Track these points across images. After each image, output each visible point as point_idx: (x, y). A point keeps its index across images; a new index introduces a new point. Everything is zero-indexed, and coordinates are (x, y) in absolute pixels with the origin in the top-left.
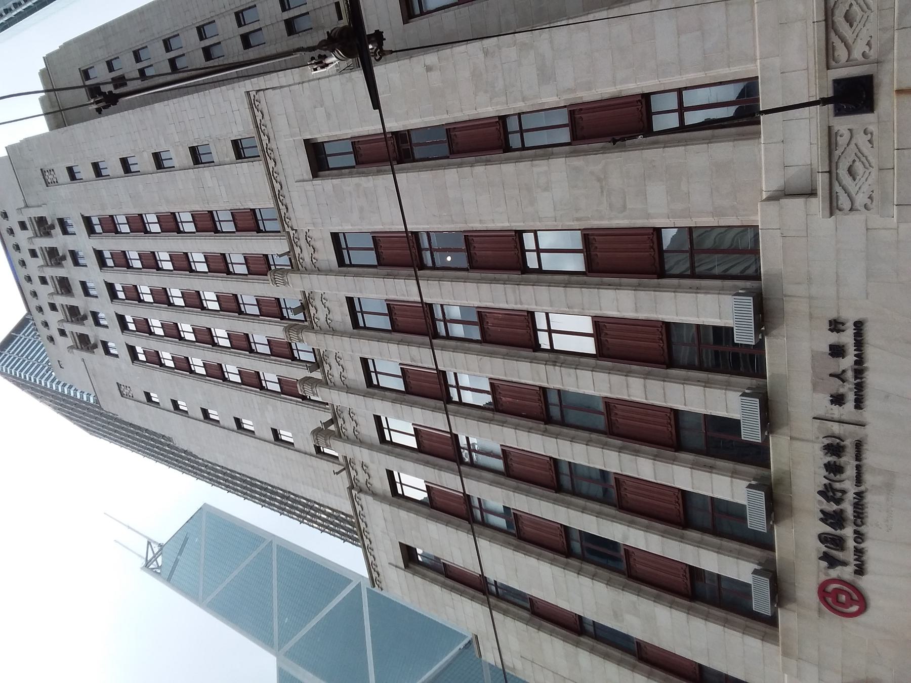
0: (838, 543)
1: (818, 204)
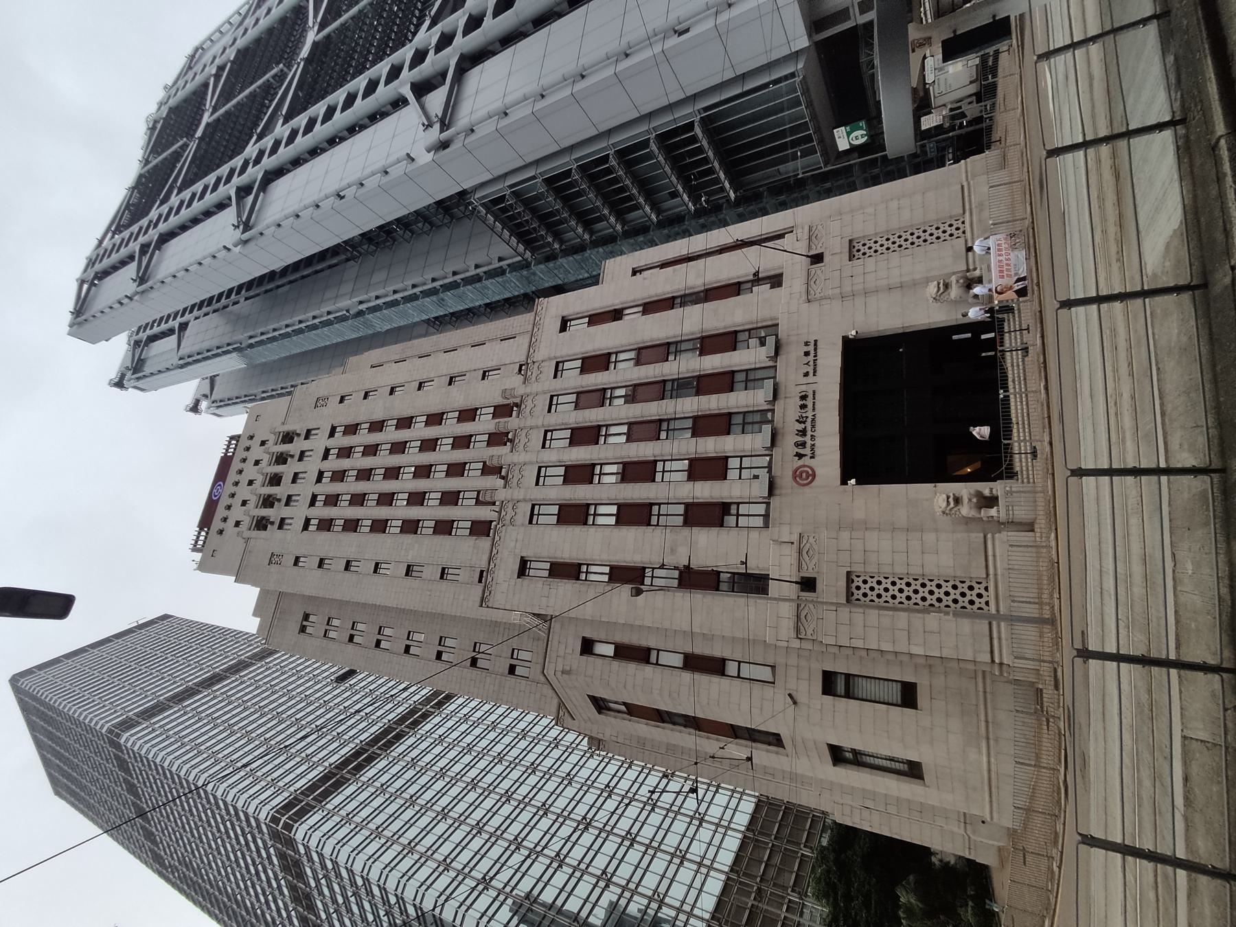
0: (803, 444)
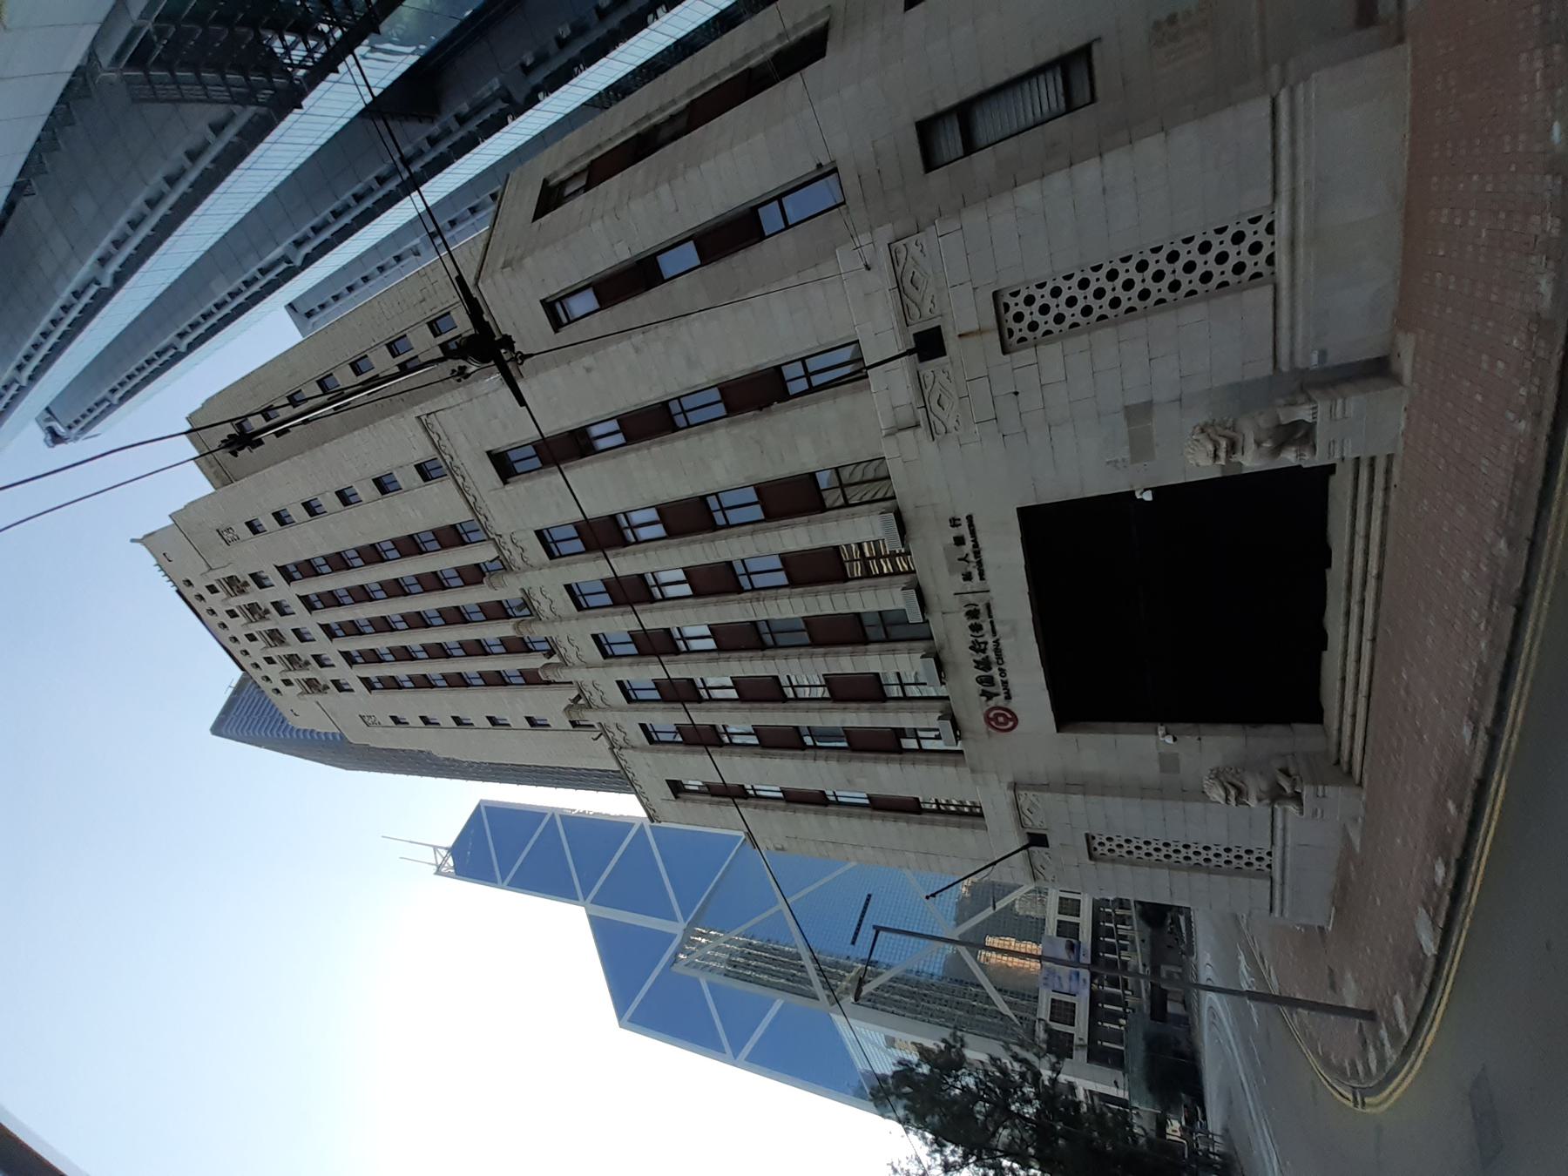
0: (990, 681)
1: (922, 432)
